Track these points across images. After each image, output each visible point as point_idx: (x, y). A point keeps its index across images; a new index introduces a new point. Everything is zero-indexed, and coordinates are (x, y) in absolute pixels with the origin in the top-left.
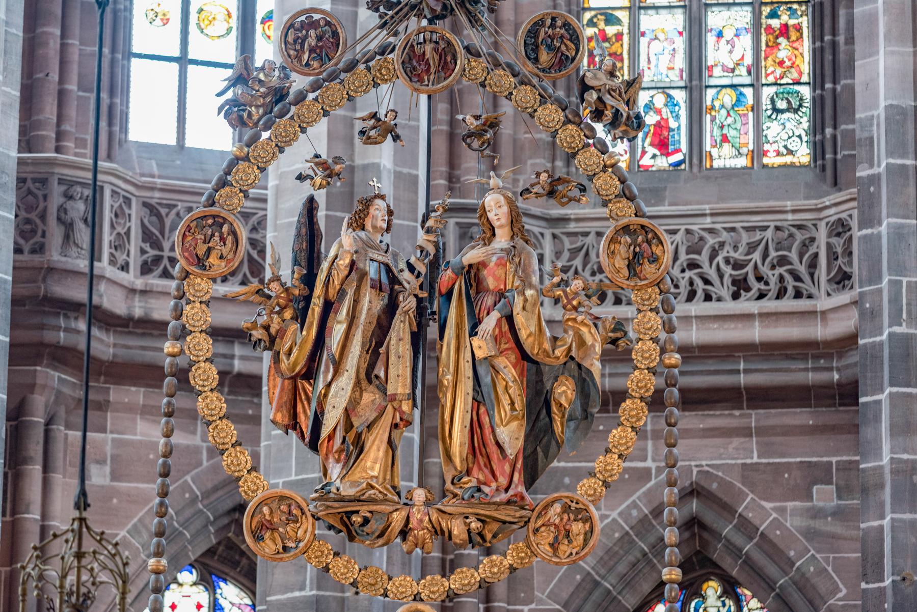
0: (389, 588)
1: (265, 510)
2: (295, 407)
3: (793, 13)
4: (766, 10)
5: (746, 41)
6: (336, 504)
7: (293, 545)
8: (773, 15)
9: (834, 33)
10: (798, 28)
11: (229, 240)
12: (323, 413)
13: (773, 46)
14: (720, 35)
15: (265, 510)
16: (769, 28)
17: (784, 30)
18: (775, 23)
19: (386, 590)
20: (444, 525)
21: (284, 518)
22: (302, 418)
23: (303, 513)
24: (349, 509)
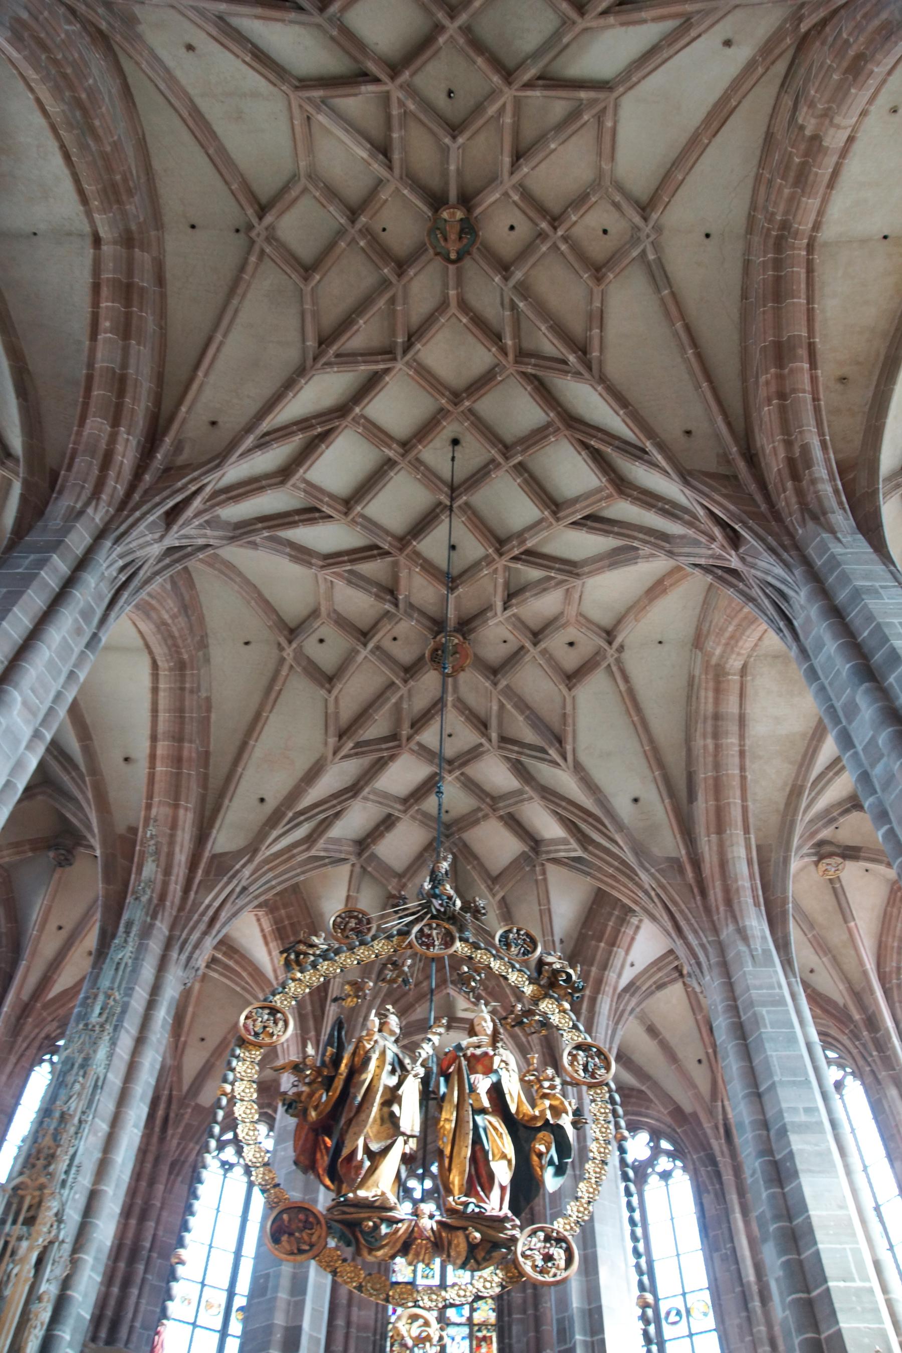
0: (391, 1293)
1: (285, 1216)
2: (314, 1154)
3: (488, 1330)
4: (476, 1328)
5: (467, 1342)
6: (352, 1210)
7: (307, 1248)
8: (479, 1330)
9: (510, 1338)
10: (491, 1337)
11: (281, 1024)
12: (343, 1143)
13: (479, 1346)
14: (453, 1339)
15: (285, 1216)
16: (477, 1337)
17: (484, 1338)
18: (480, 1335)
19: (388, 1295)
20: (444, 1234)
21: (301, 1225)
22: (320, 1162)
23: (319, 1222)
24: (362, 1215)
